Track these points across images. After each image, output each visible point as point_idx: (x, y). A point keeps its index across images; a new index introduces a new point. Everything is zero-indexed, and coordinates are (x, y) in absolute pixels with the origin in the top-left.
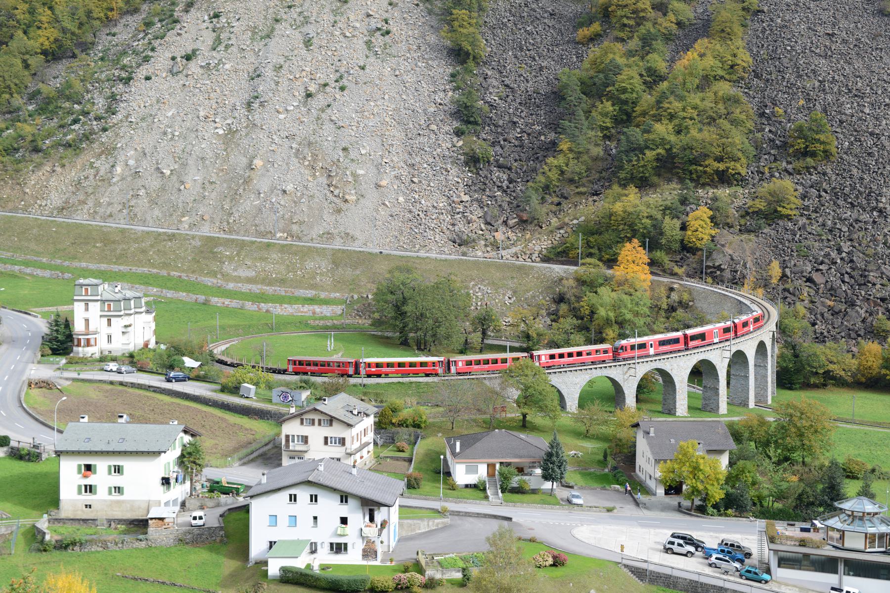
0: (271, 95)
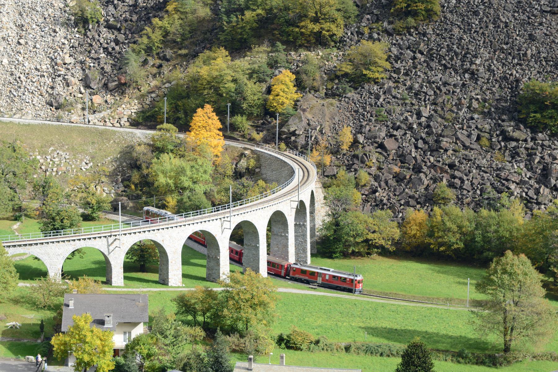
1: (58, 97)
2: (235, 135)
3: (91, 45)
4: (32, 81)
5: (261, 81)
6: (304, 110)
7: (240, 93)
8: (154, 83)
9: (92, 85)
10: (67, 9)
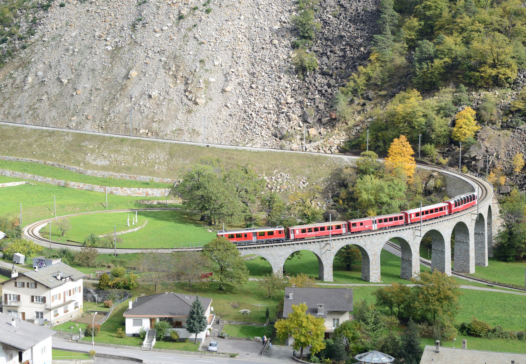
0: (152, 17)
1: (282, 130)
2: (425, 160)
3: (308, 88)
4: (261, 117)
5: (447, 116)
6: (483, 140)
7: (429, 126)
8: (359, 118)
9: (309, 120)
10: (290, 60)
